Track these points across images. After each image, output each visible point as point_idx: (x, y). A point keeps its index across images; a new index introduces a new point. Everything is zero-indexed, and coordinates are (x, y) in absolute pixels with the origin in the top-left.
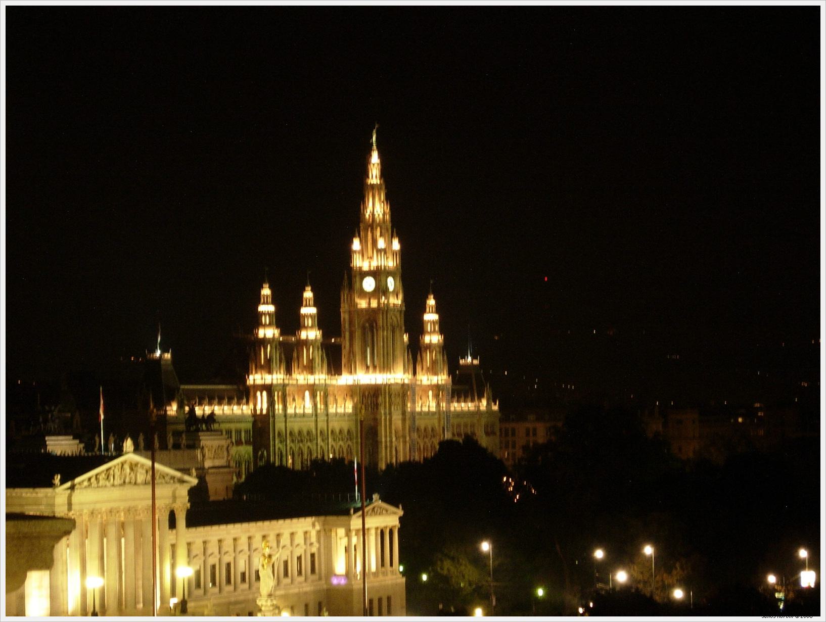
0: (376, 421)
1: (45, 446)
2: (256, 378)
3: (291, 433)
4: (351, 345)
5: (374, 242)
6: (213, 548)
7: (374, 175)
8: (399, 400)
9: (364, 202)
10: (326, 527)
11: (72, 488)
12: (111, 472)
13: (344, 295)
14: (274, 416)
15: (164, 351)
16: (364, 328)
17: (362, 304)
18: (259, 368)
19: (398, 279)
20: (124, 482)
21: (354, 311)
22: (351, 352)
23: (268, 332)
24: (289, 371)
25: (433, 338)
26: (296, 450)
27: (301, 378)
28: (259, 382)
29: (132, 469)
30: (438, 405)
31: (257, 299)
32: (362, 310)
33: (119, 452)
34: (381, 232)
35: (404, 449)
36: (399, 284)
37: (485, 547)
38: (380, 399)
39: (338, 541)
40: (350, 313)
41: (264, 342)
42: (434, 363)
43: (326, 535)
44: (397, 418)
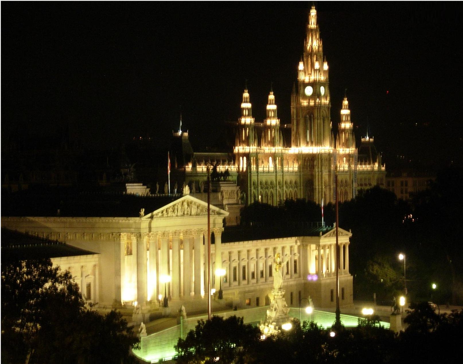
0: (313, 176)
1: (125, 190)
2: (239, 149)
3: (261, 183)
5: (313, 65)
6: (235, 256)
8: (327, 163)
9: (306, 40)
10: (304, 243)
11: (152, 217)
12: (176, 207)
13: (293, 98)
14: (250, 172)
15: (184, 131)
16: (305, 118)
17: (305, 103)
18: (241, 142)
20: (184, 214)
21: (300, 108)
22: (297, 133)
23: (247, 120)
24: (259, 144)
25: (346, 125)
26: (264, 193)
27: (267, 149)
28: (241, 151)
29: (188, 205)
30: (349, 166)
31: (240, 100)
33: (181, 194)
34: (317, 58)
35: (330, 193)
37: (401, 257)
38: (315, 163)
39: (311, 251)
41: (245, 126)
42: (347, 140)
43: (304, 248)
44: (325, 174)
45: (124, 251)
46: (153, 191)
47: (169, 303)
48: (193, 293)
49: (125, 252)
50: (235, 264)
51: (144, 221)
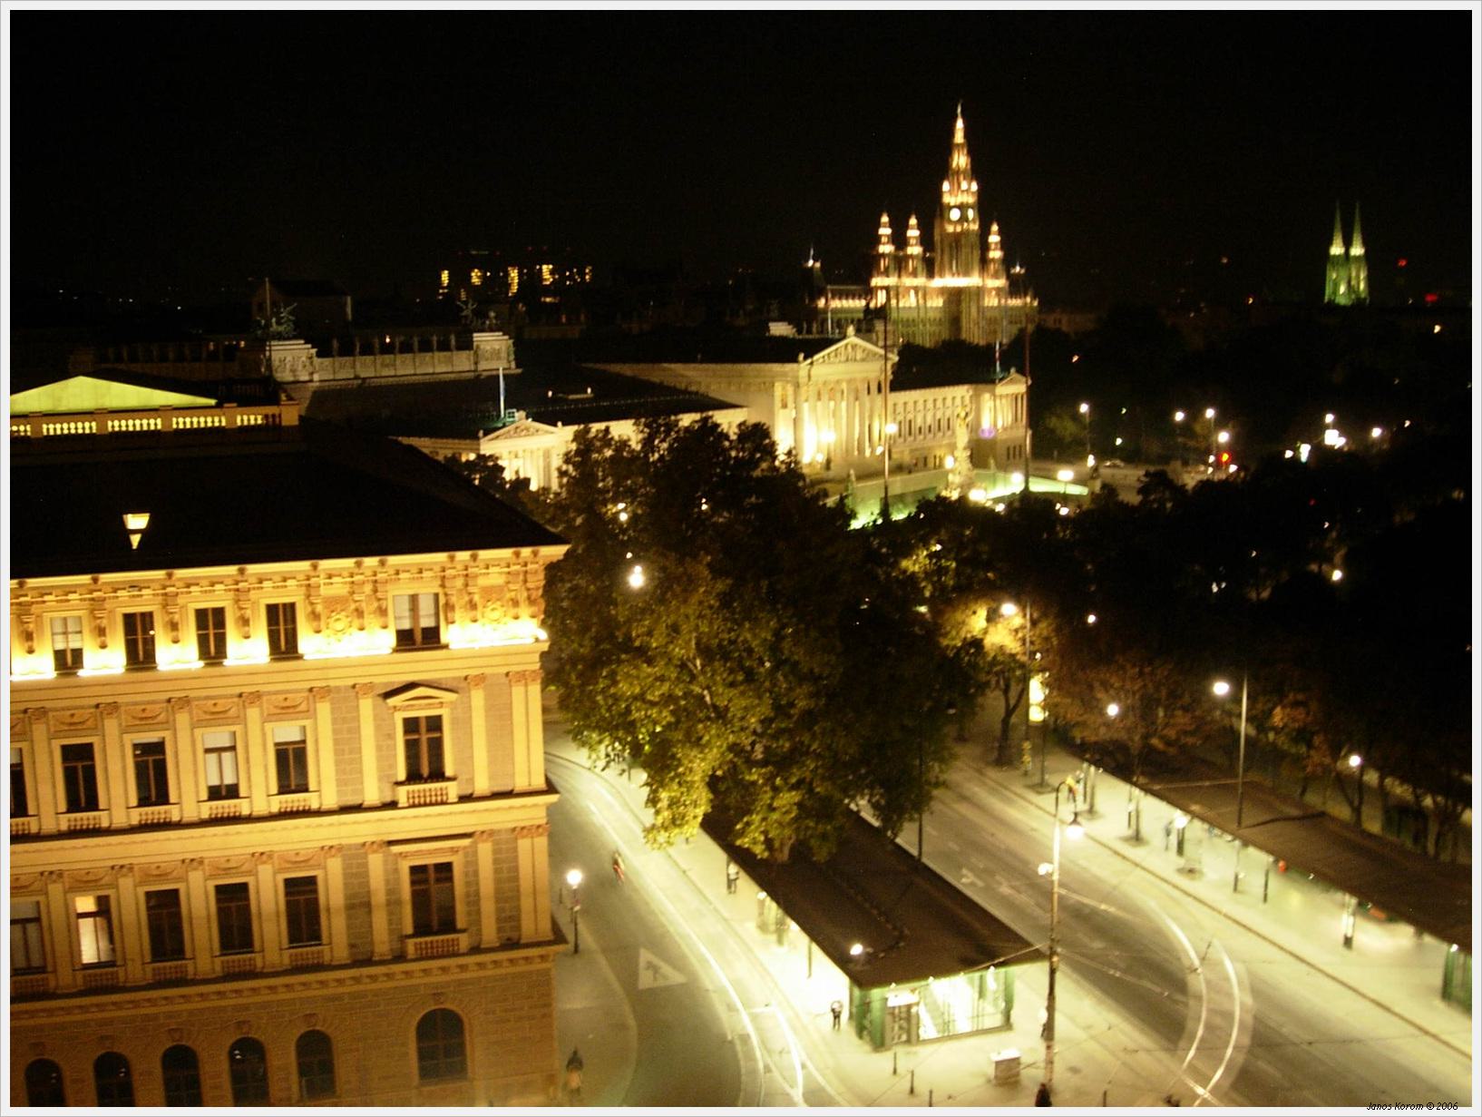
0: (960, 312)
2: (876, 281)
4: (942, 259)
6: (900, 409)
7: (959, 137)
8: (975, 298)
11: (812, 363)
13: (937, 224)
16: (951, 247)
17: (950, 229)
18: (880, 274)
21: (944, 234)
23: (886, 248)
24: (899, 276)
25: (995, 254)
27: (908, 281)
28: (879, 284)
31: (878, 225)
32: (949, 234)
33: (844, 337)
36: (977, 217)
37: (1084, 408)
38: (963, 297)
40: (941, 235)
41: (883, 255)
44: (974, 310)
45: (778, 403)
46: (799, 332)
47: (832, 465)
48: (856, 453)
49: (780, 405)
50: (900, 418)
51: (802, 367)
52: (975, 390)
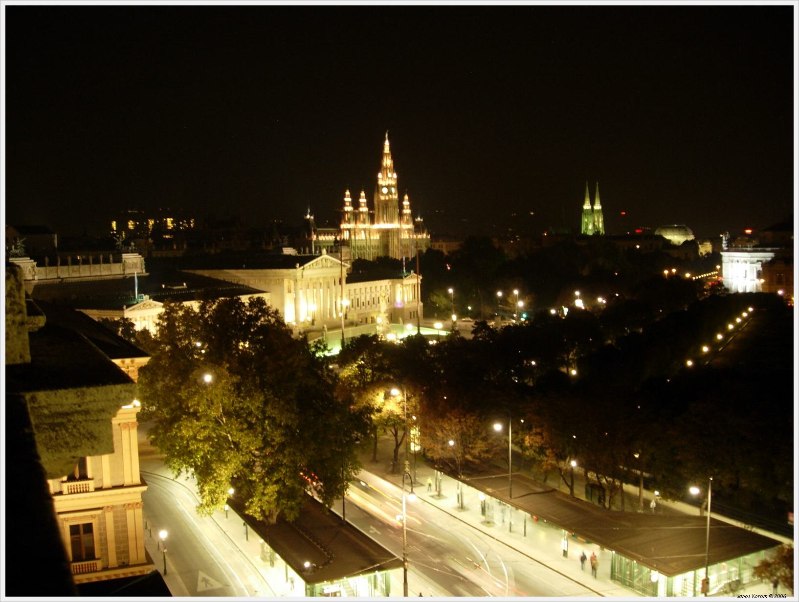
0: (388, 242)
1: (282, 251)
2: (344, 226)
3: (357, 247)
4: (378, 213)
6: (352, 292)
7: (387, 150)
11: (303, 269)
12: (318, 262)
13: (376, 195)
14: (351, 240)
15: (311, 215)
16: (383, 207)
17: (382, 198)
18: (345, 222)
19: (396, 189)
20: (323, 267)
21: (380, 201)
22: (379, 216)
24: (356, 223)
25: (407, 211)
26: (359, 253)
27: (360, 226)
28: (345, 227)
29: (325, 261)
30: (409, 236)
31: (344, 196)
32: (383, 200)
33: (321, 254)
35: (398, 252)
36: (397, 191)
37: (451, 291)
38: (390, 234)
40: (378, 202)
41: (347, 212)
42: (407, 220)
43: (393, 286)
44: (396, 241)
45: (286, 290)
46: (299, 253)
47: (315, 323)
48: (329, 316)
49: (287, 291)
50: (352, 297)
51: (298, 271)
52: (392, 283)
